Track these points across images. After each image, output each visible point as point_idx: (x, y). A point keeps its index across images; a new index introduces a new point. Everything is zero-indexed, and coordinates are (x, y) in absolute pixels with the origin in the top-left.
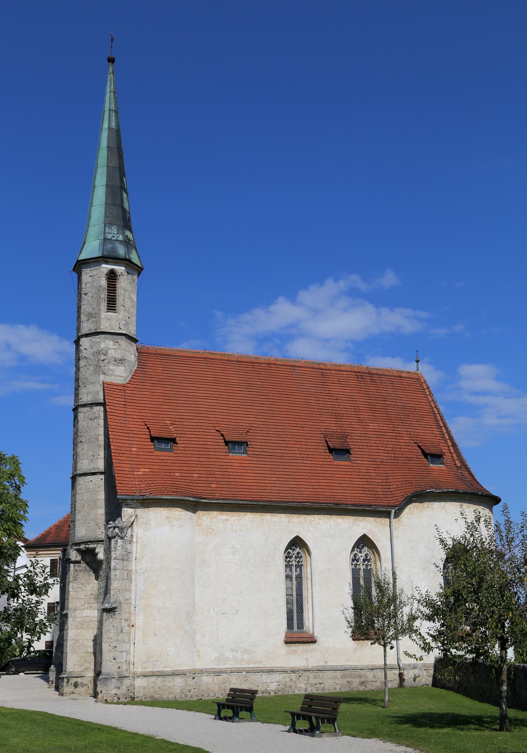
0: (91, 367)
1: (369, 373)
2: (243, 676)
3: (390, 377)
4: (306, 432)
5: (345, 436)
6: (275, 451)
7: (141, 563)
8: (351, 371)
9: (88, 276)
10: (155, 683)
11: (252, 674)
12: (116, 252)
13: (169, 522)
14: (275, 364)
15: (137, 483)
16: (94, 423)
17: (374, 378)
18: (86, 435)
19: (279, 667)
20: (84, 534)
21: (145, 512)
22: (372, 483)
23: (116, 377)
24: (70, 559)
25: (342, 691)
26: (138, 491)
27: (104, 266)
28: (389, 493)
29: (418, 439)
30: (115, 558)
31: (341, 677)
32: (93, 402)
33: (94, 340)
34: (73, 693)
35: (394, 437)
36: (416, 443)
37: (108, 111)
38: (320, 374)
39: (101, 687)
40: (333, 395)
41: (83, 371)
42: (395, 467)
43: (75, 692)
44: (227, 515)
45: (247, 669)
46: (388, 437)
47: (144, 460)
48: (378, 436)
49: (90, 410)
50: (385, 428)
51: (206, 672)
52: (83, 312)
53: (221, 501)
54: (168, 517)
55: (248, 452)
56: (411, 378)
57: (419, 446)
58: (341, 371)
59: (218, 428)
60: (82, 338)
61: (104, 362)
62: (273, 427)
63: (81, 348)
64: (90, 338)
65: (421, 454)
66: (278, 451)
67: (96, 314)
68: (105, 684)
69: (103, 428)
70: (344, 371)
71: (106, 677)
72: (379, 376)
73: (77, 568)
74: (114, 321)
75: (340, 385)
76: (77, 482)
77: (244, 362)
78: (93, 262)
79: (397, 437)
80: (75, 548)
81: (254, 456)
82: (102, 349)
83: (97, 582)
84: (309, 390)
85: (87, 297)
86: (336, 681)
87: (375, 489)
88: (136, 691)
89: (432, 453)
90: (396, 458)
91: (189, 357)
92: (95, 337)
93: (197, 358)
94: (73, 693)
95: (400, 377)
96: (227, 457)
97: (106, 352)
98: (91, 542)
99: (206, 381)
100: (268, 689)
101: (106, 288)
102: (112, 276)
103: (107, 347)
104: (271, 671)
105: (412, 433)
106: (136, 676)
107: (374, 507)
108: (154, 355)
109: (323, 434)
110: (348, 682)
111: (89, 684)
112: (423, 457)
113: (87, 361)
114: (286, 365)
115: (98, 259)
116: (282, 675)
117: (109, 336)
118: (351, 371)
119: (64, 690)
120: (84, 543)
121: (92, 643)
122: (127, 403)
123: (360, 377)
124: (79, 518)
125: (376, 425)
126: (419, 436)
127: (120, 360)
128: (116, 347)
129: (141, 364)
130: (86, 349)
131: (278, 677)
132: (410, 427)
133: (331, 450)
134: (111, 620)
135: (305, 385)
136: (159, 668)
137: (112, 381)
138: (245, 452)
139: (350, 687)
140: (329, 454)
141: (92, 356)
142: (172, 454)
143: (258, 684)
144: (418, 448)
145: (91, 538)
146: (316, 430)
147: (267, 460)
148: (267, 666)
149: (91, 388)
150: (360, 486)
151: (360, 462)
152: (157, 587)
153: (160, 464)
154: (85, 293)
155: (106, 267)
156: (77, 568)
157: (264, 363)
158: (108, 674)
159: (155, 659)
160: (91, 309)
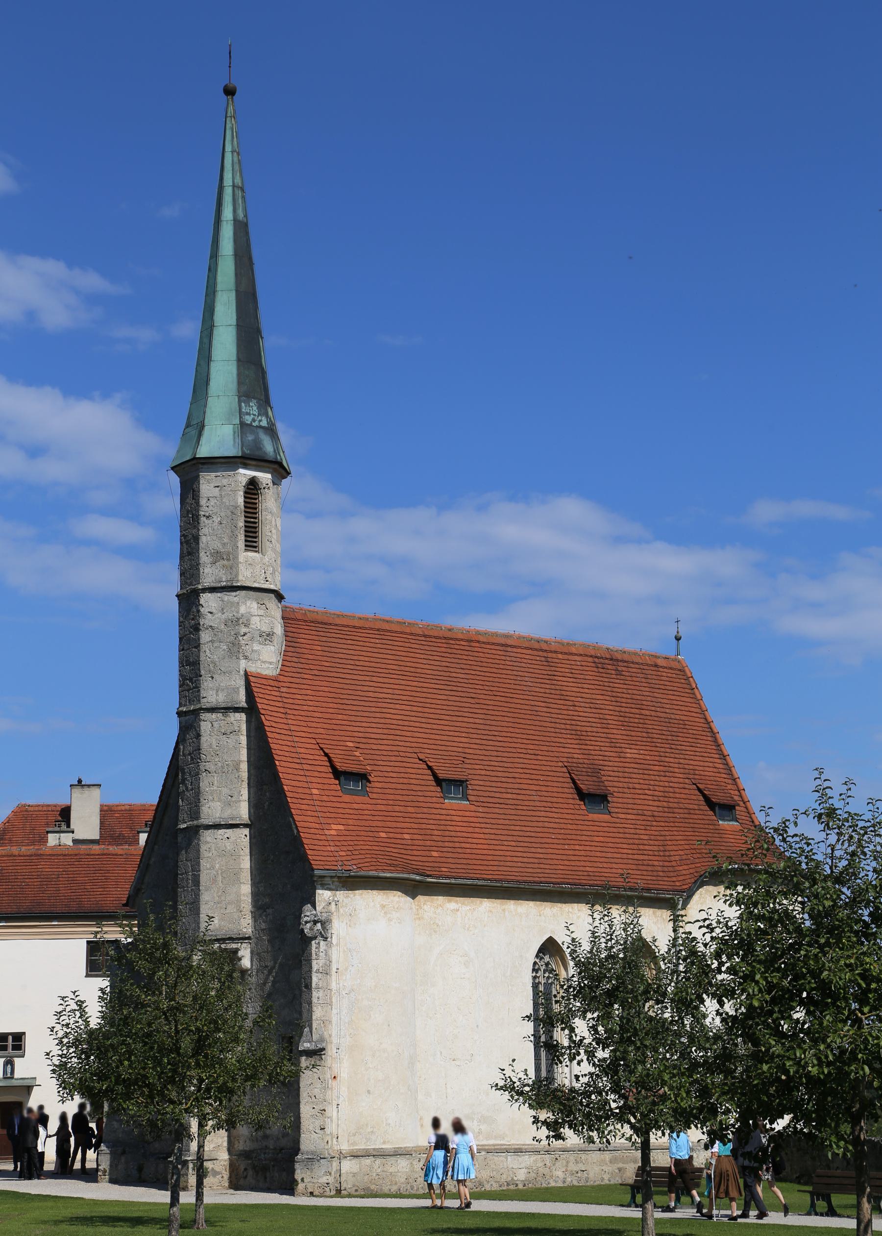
0: (222, 644)
1: (611, 659)
2: (482, 1158)
3: (642, 667)
4: (541, 763)
5: (595, 771)
6: (505, 796)
7: (344, 978)
8: (586, 656)
9: (212, 485)
10: (371, 1167)
11: (494, 1155)
12: (260, 449)
13: (385, 913)
14: (478, 642)
15: (333, 849)
16: (231, 741)
17: (620, 668)
18: (217, 760)
19: (529, 1145)
20: (217, 925)
21: (347, 897)
22: (645, 852)
23: (263, 664)
25: (612, 1183)
26: (340, 863)
27: (242, 471)
28: (671, 869)
29: (696, 777)
30: (318, 971)
31: (611, 1162)
32: (229, 705)
33: (226, 598)
35: (662, 773)
36: (694, 784)
37: (230, 189)
38: (543, 659)
39: (302, 1173)
40: (567, 698)
41: (208, 651)
42: (672, 824)
44: (457, 902)
45: (487, 1147)
46: (655, 773)
47: (332, 810)
48: (641, 771)
49: (223, 718)
50: (648, 757)
52: (203, 548)
53: (453, 881)
54: (384, 907)
55: (471, 798)
56: (671, 668)
57: (699, 790)
58: (572, 654)
59: (422, 756)
60: (204, 593)
61: (245, 638)
62: (495, 753)
63: (202, 610)
64: (219, 594)
65: (704, 803)
66: (509, 796)
67: (228, 554)
68: (309, 1167)
69: (246, 750)
70: (576, 655)
71: (310, 1157)
72: (625, 664)
74: (258, 567)
75: (574, 680)
76: (201, 838)
77: (435, 637)
79: (667, 774)
81: (478, 804)
82: (242, 616)
84: (533, 689)
85: (210, 521)
86: (603, 1168)
87: (650, 863)
88: (343, 1179)
89: (722, 802)
90: (671, 810)
91: (354, 627)
92: (228, 593)
93: (366, 629)
95: (656, 666)
96: (443, 806)
97: (248, 620)
98: (231, 939)
99: (387, 671)
100: (515, 1179)
101: (243, 508)
102: (253, 488)
103: (249, 613)
105: (686, 766)
106: (342, 1156)
107: (654, 893)
108: (304, 623)
109: (566, 766)
110: (620, 1170)
111: (224, 1172)
112: (707, 808)
114: (493, 644)
115: (232, 460)
116: (534, 1157)
117: (251, 593)
118: (586, 656)
119: (189, 1181)
120: (218, 940)
122: (289, 711)
123: (600, 665)
124: (207, 899)
125: (635, 751)
126: (697, 772)
127: (268, 635)
128: (261, 612)
129: (290, 639)
130: (211, 613)
131: (527, 1160)
132: (682, 756)
133: (582, 796)
135: (527, 679)
136: (376, 1145)
137: (259, 671)
138: (465, 797)
139: (621, 1177)
140: (578, 802)
141: (223, 626)
142: (366, 799)
143: (502, 1171)
144: (697, 792)
146: (555, 759)
147: (497, 811)
148: (512, 1142)
149: (222, 681)
150: (630, 856)
151: (623, 816)
152: (370, 1016)
153: (356, 817)
154: (207, 514)
155: (245, 474)
157: (462, 640)
158: (313, 1153)
159: (369, 1130)
160: (219, 545)
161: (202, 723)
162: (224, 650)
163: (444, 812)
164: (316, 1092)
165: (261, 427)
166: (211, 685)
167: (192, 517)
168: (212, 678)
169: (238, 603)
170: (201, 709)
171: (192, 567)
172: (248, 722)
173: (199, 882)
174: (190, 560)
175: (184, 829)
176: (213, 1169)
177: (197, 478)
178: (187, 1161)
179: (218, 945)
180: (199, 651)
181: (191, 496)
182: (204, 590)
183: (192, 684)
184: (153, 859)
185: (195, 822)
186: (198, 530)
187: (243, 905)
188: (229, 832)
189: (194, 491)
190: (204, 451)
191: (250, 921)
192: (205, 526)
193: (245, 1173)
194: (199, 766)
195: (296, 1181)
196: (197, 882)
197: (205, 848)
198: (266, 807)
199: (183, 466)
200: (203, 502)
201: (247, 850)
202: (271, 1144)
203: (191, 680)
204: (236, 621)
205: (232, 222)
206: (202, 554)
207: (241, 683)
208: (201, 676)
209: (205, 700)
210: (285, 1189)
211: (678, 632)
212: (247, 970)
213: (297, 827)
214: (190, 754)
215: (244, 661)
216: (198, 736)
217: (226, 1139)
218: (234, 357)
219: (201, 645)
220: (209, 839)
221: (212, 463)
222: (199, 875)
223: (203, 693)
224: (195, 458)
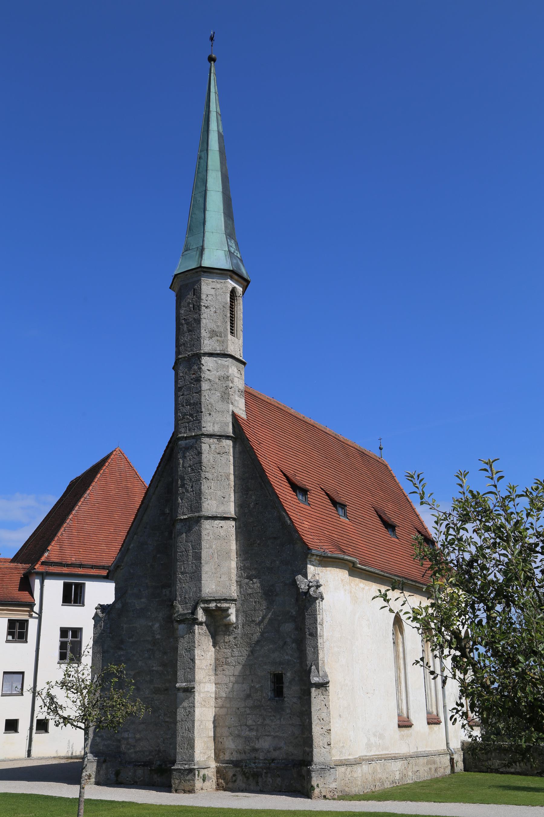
0: (217, 392)
18: (213, 471)
20: (214, 590)
21: (322, 572)
24: (197, 619)
27: (229, 280)
32: (223, 434)
33: (220, 362)
34: (202, 789)
39: (317, 780)
41: (207, 395)
43: (204, 788)
51: (363, 760)
52: (204, 327)
60: (204, 356)
63: (203, 368)
64: (215, 359)
67: (221, 333)
73: (200, 631)
76: (202, 526)
78: (217, 273)
80: (202, 605)
83: (214, 649)
86: (425, 768)
92: (221, 359)
94: (202, 789)
98: (226, 600)
104: (395, 758)
111: (213, 777)
113: (212, 385)
115: (225, 272)
119: (196, 785)
120: (216, 600)
121: (212, 726)
124: (206, 570)
130: (209, 370)
134: (322, 697)
138: (345, 515)
141: (217, 380)
145: (225, 596)
149: (217, 417)
152: (339, 660)
154: (207, 305)
155: (231, 284)
156: (200, 631)
159: (341, 745)
161: (203, 445)
162: (218, 396)
164: (324, 715)
166: (209, 419)
167: (194, 307)
168: (210, 414)
169: (228, 366)
170: (203, 434)
171: (192, 339)
172: (234, 447)
173: (201, 557)
174: (191, 335)
175: (184, 519)
176: (208, 774)
177: (199, 282)
178: (194, 769)
179: (215, 604)
180: (200, 395)
181: (191, 293)
182: (205, 354)
183: (193, 418)
184: (132, 545)
185: (197, 514)
186: (200, 315)
187: (232, 576)
188: (222, 523)
189: (194, 290)
190: (207, 263)
191: (236, 588)
192: (205, 313)
193: (234, 778)
194: (200, 474)
195: (312, 786)
196: (198, 557)
197: (205, 533)
198: (251, 506)
199: (187, 273)
200: (203, 297)
201: (234, 537)
202: (261, 756)
203: (191, 415)
204: (227, 378)
205: (217, 132)
206: (202, 331)
207: (230, 419)
208: (202, 412)
210: (280, 791)
212: (233, 624)
213: (290, 519)
214: (190, 466)
215: (231, 405)
216: (200, 453)
217: (213, 751)
218: (222, 211)
219: (202, 391)
220: (208, 527)
221: (210, 273)
222: (201, 553)
223: (203, 424)
224: (201, 267)
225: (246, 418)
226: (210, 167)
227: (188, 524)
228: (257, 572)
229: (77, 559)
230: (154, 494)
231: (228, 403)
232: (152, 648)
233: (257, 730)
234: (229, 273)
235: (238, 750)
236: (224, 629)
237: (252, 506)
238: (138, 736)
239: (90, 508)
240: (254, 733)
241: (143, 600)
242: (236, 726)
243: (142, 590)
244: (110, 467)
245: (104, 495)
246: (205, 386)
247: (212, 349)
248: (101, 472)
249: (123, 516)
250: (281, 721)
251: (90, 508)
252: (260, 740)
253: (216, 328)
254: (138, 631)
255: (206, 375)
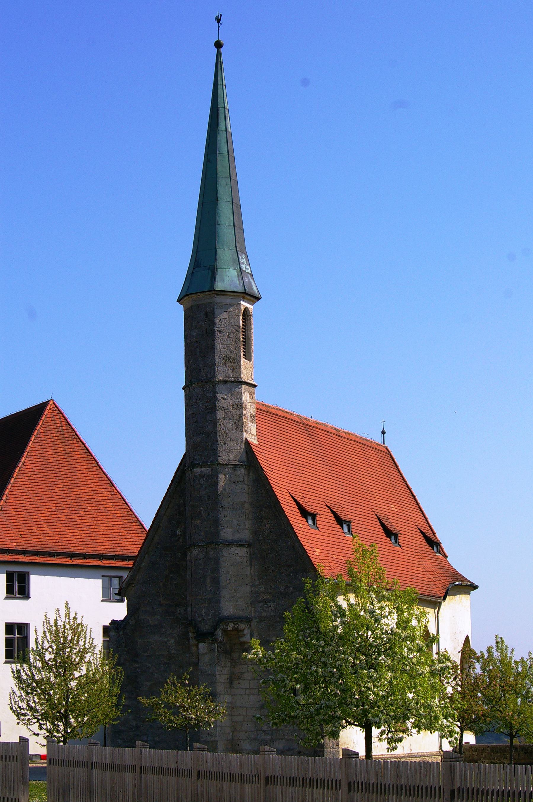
27: (242, 303)
63: (218, 396)
67: (234, 359)
78: (229, 295)
85: (222, 335)
97: (246, 405)
154: (220, 330)
163: (345, 542)
165: (248, 273)
186: (213, 341)
190: (219, 286)
198: (266, 534)
206: (217, 357)
209: (219, 458)
211: (383, 429)
220: (224, 554)
221: (223, 295)
225: (257, 443)
226: (220, 174)
227: (205, 550)
228: (272, 597)
229: (19, 544)
230: (165, 514)
231: (242, 431)
232: (168, 662)
233: (272, 734)
234: (241, 295)
235: (254, 750)
236: (239, 647)
237: (266, 533)
238: (157, 739)
239: (26, 480)
240: (269, 737)
241: (156, 617)
242: (252, 731)
243: (155, 608)
244: (45, 426)
245: (40, 463)
246: (220, 415)
247: (226, 375)
248: (36, 433)
249: (64, 489)
250: (294, 727)
251: (26, 480)
252: (274, 742)
253: (229, 353)
254: (152, 646)
255: (222, 403)
